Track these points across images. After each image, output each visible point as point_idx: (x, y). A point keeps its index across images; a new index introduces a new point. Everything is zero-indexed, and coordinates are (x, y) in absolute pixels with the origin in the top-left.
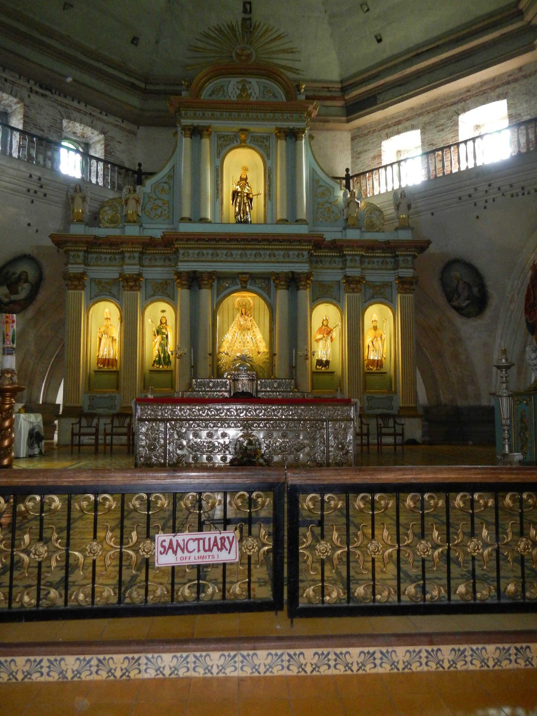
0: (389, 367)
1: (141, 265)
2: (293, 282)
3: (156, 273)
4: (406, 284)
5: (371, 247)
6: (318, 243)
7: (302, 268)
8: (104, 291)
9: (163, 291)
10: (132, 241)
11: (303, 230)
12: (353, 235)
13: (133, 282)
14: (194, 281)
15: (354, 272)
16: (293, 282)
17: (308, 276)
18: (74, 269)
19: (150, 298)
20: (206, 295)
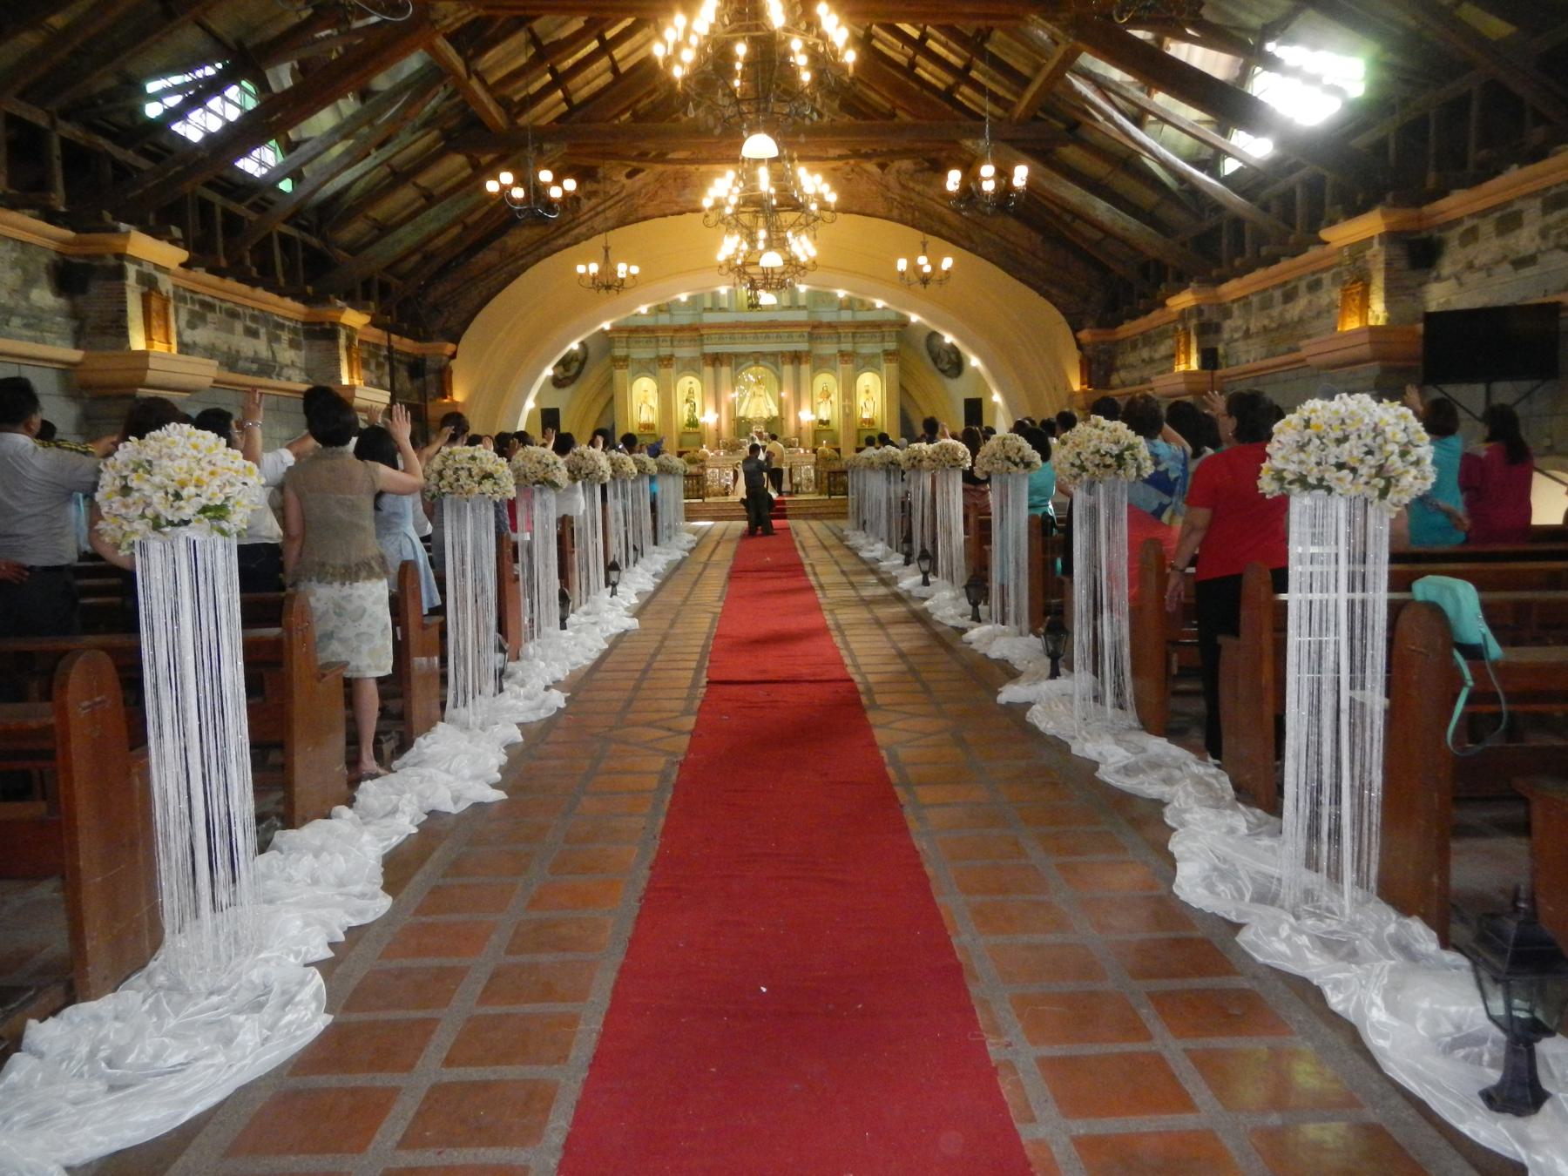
1: (672, 345)
3: (685, 352)
4: (888, 354)
6: (816, 326)
7: (803, 346)
8: (646, 368)
9: (691, 367)
10: (665, 329)
11: (802, 316)
12: (846, 316)
13: (667, 361)
14: (716, 360)
16: (796, 358)
17: (808, 353)
18: (619, 352)
20: (725, 371)
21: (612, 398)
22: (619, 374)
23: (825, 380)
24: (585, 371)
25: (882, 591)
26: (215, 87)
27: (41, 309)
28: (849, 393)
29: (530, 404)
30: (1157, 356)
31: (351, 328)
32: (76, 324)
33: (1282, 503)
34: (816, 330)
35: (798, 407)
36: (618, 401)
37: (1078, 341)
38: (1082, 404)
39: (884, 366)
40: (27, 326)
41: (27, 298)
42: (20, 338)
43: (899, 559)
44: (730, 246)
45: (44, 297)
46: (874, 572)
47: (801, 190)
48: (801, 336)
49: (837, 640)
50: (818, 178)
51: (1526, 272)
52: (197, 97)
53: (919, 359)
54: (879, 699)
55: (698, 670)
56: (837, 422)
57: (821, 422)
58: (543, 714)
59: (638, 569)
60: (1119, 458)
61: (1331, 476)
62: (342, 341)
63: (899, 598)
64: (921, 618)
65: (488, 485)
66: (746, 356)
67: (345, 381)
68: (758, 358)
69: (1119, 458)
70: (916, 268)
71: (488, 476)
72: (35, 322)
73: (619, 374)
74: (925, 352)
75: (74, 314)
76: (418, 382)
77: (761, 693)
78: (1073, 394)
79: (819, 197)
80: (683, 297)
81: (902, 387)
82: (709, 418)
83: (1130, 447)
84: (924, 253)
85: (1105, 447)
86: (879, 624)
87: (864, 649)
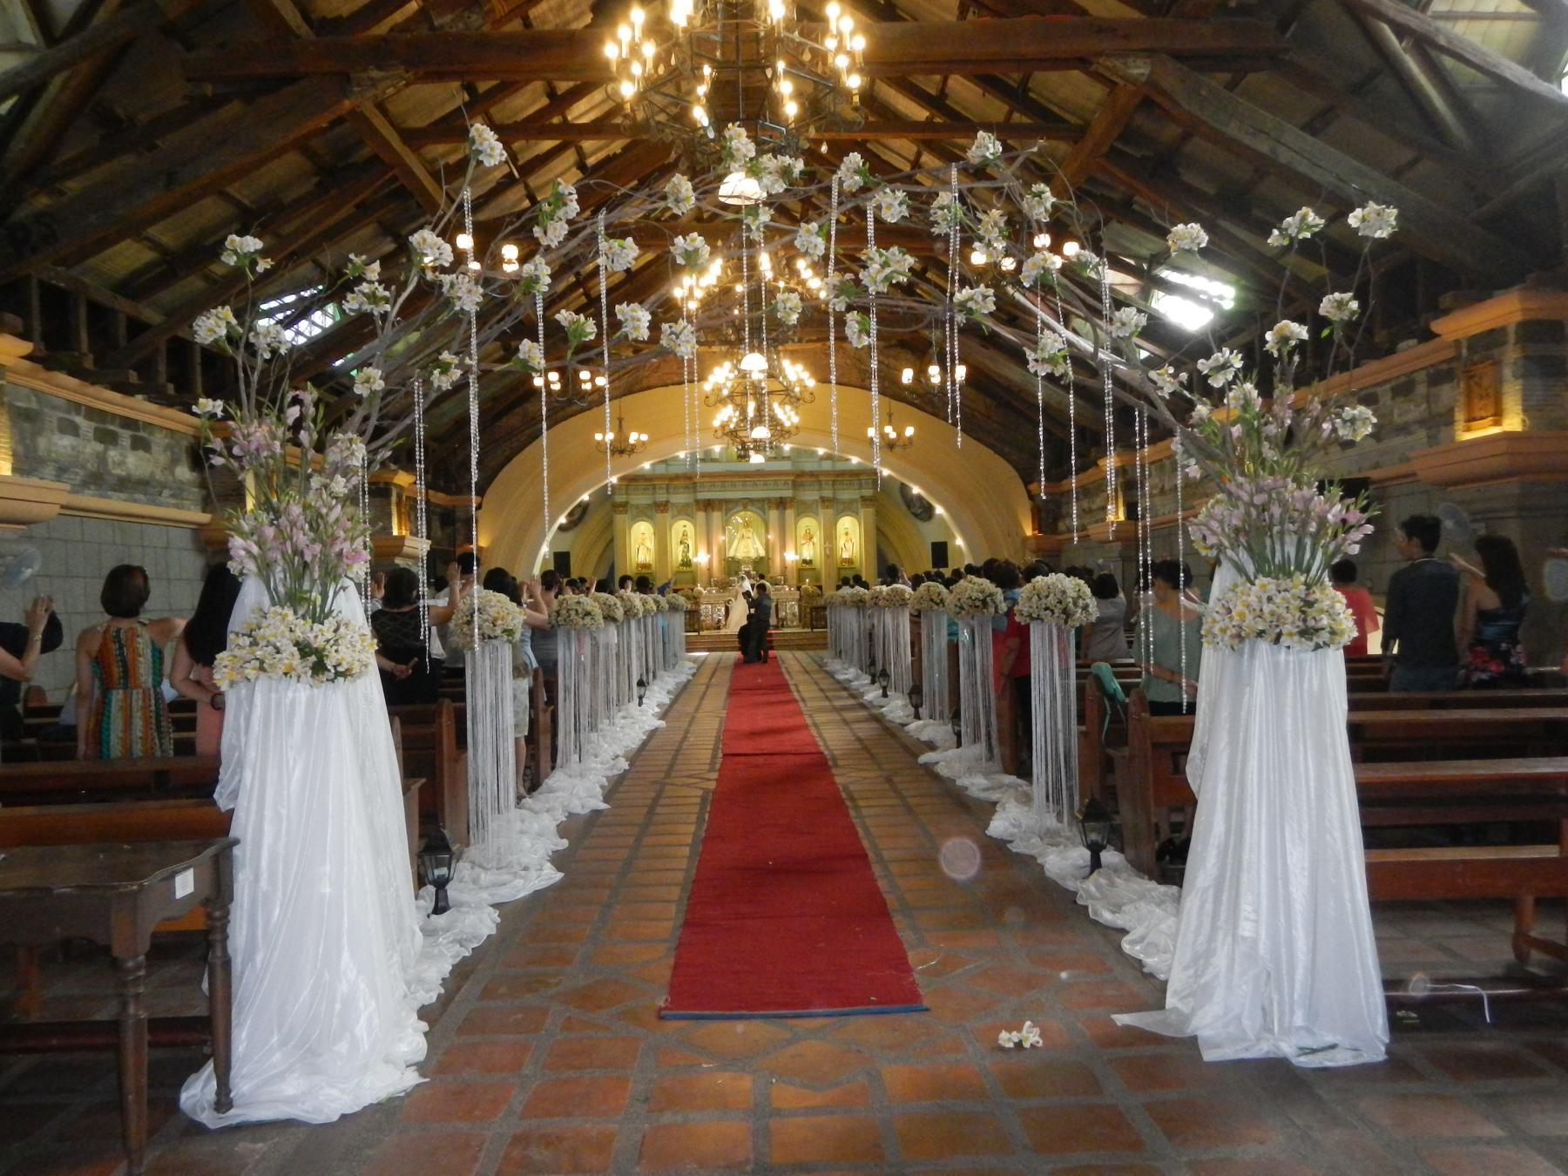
0: (857, 564)
2: (781, 504)
3: (680, 498)
5: (842, 474)
6: (801, 474)
7: (788, 493)
9: (685, 512)
11: (786, 466)
12: (827, 466)
13: (663, 507)
14: (708, 505)
15: (828, 493)
16: (781, 504)
17: (792, 499)
18: (619, 499)
19: (675, 517)
20: (717, 516)
21: (612, 540)
22: (619, 518)
23: (808, 523)
24: (587, 517)
25: (851, 702)
26: (318, 303)
27: (182, 482)
28: (830, 537)
29: (545, 549)
30: (1094, 507)
31: (400, 487)
32: (204, 492)
33: (1027, 627)
34: (800, 478)
35: (783, 548)
36: (618, 542)
37: (1029, 492)
38: (1033, 546)
39: (862, 511)
40: (173, 496)
41: (173, 473)
42: (168, 505)
43: (867, 679)
44: (726, 415)
45: (184, 472)
46: (845, 689)
47: (785, 377)
48: (786, 483)
49: (814, 732)
50: (799, 367)
51: (1350, 452)
52: (303, 311)
53: (890, 508)
54: (840, 763)
55: (715, 750)
56: (819, 561)
57: (805, 561)
58: (616, 772)
59: (656, 688)
60: (984, 602)
61: (1043, 613)
62: (394, 498)
63: (863, 706)
64: (878, 719)
65: (588, 619)
66: (736, 502)
67: (395, 532)
68: (746, 503)
69: (984, 602)
70: (883, 436)
71: (588, 614)
72: (178, 492)
73: (619, 518)
74: (899, 499)
75: (203, 485)
76: (449, 530)
77: (761, 760)
78: (1025, 539)
79: (800, 381)
80: (682, 455)
81: (878, 529)
82: (701, 558)
83: (991, 595)
84: (890, 423)
85: (974, 595)
86: (846, 722)
87: (831, 734)
